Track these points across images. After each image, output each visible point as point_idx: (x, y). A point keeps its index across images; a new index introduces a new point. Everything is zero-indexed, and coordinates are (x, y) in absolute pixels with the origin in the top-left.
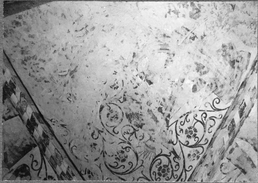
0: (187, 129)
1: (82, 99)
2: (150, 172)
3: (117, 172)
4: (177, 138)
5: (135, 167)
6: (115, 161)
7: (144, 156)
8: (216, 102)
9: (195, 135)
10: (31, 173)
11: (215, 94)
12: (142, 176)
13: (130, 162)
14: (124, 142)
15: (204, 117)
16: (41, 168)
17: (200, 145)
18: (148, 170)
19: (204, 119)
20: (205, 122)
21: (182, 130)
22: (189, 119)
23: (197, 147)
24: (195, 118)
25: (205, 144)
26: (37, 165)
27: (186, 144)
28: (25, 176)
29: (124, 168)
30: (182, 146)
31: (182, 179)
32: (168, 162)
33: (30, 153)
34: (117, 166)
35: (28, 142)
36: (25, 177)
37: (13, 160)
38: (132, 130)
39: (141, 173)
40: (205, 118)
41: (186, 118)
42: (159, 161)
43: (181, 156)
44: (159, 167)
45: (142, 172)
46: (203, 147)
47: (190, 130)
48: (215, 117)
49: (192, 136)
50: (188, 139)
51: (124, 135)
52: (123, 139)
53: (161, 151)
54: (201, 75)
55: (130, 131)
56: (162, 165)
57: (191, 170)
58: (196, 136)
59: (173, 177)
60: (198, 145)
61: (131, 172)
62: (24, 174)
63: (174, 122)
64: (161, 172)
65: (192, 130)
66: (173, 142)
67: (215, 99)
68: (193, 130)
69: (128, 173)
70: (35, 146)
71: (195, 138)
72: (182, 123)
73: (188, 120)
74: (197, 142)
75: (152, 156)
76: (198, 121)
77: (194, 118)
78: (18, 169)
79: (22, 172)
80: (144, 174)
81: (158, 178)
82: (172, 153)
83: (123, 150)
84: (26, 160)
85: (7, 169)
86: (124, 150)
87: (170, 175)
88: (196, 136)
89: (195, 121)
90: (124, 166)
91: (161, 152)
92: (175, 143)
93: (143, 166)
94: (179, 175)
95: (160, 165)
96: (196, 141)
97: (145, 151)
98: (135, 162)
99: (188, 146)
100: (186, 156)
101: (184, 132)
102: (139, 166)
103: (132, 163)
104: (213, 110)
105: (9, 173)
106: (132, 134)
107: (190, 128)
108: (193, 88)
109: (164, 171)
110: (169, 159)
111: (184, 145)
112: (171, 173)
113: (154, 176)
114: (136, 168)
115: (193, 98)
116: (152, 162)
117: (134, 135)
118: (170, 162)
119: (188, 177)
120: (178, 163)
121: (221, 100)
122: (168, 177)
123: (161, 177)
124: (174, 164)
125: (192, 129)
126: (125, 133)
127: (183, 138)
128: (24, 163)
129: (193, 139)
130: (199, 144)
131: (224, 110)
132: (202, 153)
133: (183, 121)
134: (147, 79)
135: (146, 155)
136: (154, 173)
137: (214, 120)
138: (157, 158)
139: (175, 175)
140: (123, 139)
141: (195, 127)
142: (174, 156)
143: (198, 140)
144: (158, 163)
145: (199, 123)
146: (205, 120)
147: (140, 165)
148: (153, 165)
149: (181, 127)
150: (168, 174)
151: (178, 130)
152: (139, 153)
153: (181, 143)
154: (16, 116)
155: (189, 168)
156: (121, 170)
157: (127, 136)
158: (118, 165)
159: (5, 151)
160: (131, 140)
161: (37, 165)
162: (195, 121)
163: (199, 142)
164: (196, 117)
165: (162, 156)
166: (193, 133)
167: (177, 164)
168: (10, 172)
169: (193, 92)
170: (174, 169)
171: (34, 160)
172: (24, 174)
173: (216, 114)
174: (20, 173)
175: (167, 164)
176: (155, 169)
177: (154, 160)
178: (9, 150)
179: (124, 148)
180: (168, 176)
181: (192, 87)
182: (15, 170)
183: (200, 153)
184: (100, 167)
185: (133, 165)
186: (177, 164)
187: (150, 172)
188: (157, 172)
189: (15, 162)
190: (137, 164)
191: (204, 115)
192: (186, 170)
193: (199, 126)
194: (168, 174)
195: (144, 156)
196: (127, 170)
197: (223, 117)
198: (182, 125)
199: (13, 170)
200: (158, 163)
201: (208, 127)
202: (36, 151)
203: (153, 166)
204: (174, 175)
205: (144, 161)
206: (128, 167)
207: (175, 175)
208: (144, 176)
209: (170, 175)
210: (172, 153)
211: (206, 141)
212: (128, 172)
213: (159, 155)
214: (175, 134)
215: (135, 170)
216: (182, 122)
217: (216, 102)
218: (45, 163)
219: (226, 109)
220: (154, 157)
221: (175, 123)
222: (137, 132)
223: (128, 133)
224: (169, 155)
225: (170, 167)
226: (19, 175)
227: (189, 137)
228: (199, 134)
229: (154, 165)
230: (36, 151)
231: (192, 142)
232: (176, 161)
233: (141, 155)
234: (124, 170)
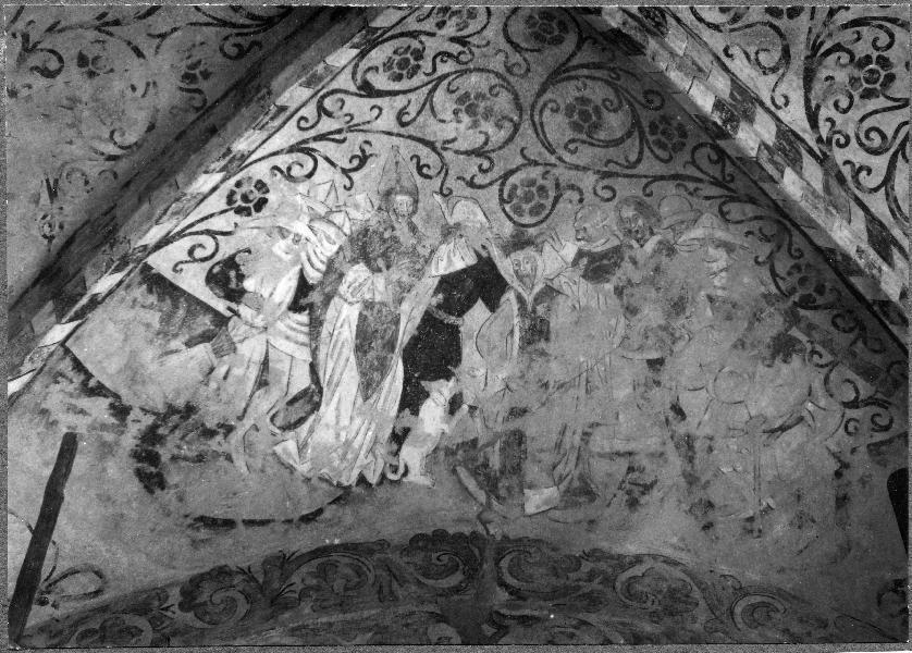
10: (227, 256)
16: (208, 232)
26: (201, 245)
28: (236, 267)
33: (169, 275)
35: (139, 292)
36: (242, 268)
62: (232, 274)
70: (147, 268)
78: (222, 294)
79: (228, 279)
84: (193, 281)
85: (231, 324)
105: (239, 316)
128: (204, 283)
159: (184, 347)
161: (201, 245)
168: (236, 313)
171: (189, 259)
172: (232, 274)
174: (233, 285)
178: (175, 336)
182: (228, 303)
184: (163, 36)
189: (208, 309)
199: (229, 309)
218: (192, 225)
226: (238, 286)
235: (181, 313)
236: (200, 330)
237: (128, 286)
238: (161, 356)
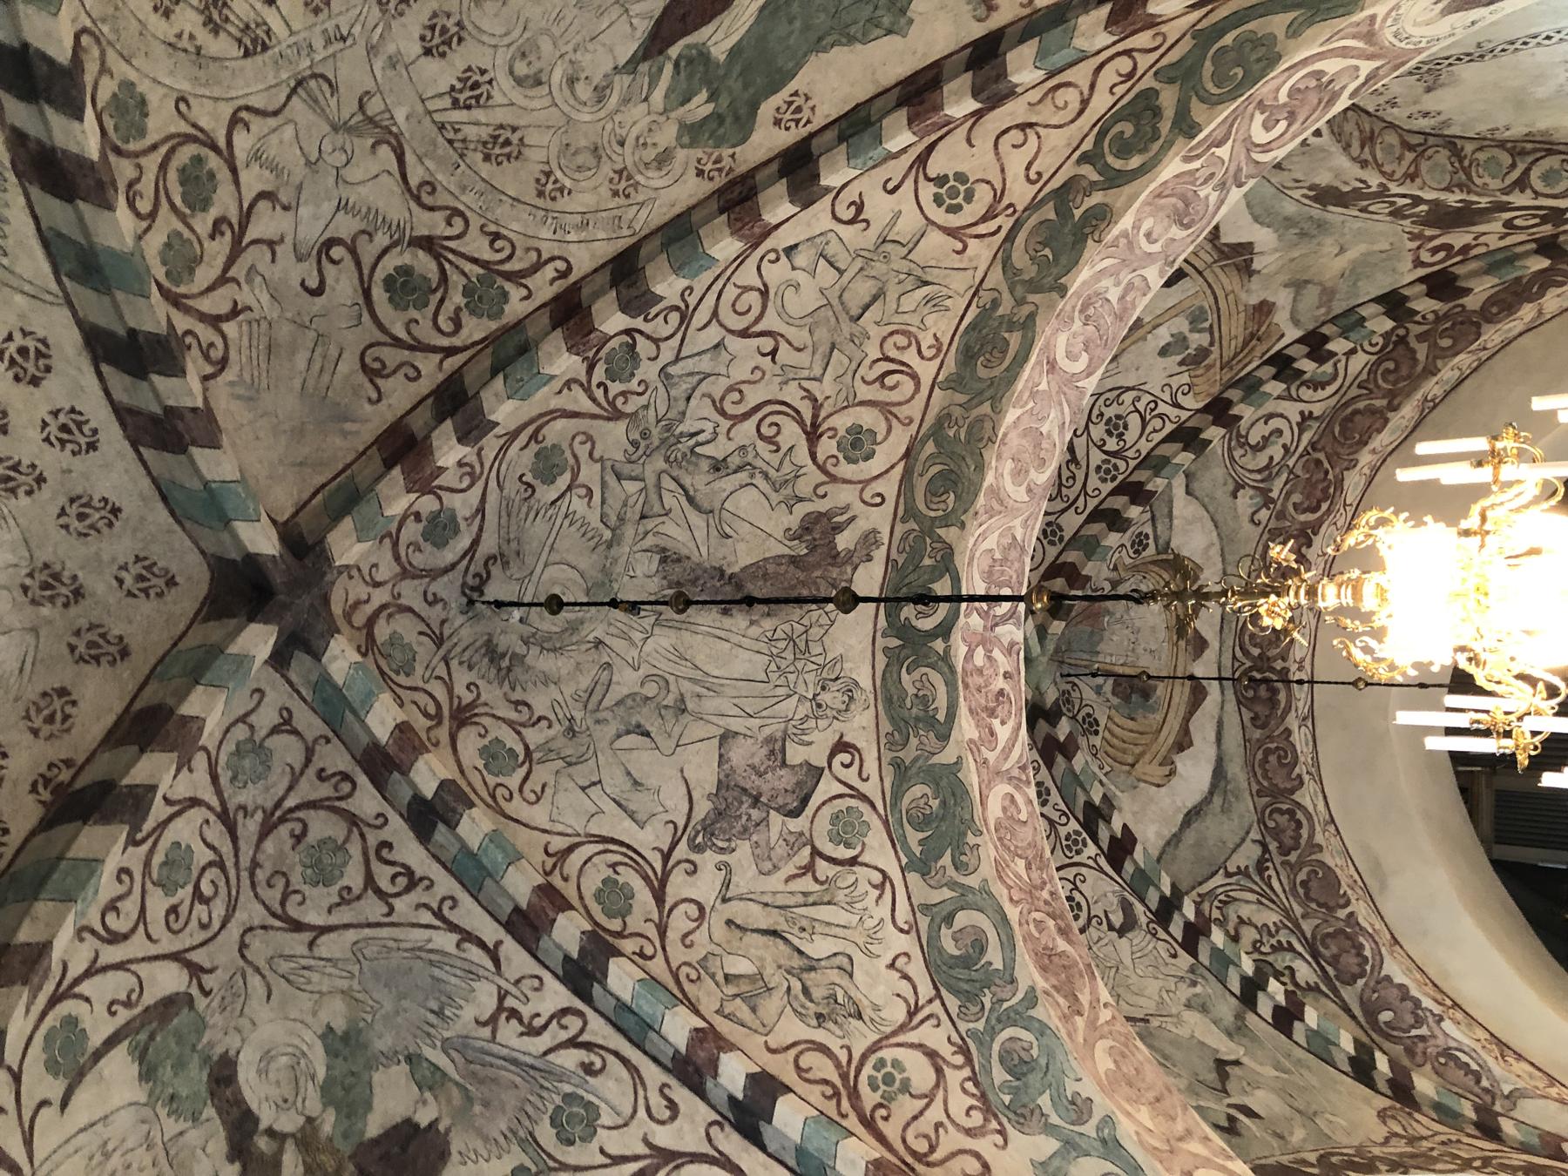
21: (1101, 415)
43: (1084, 464)
50: (1105, 437)
54: (1191, 331)
76: (1137, 411)
94: (1072, 498)
100: (1093, 466)
107: (1118, 417)
119: (1090, 508)
129: (1114, 440)
149: (1103, 409)
151: (1095, 412)
173: (1172, 412)
181: (1162, 343)
191: (1152, 405)
192: (1086, 494)
193: (1134, 421)
201: (1149, 429)
227: (1109, 433)
228: (1131, 435)
231: (1112, 445)
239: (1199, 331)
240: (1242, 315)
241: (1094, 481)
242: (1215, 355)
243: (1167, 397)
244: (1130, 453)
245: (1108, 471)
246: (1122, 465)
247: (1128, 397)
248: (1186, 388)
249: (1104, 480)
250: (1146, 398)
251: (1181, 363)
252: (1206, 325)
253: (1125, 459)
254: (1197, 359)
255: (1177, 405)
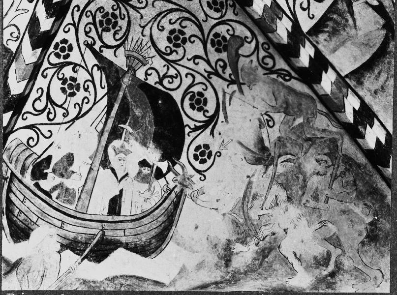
0: (78, 91)
1: (249, 121)
2: (129, 18)
3: (179, 12)
4: (92, 75)
5: (153, 23)
6: (185, 30)
7: (141, 43)
8: (33, 141)
9: (64, 81)
11: (36, 153)
12: (142, 11)
13: (161, 31)
14: (174, 62)
15: (52, 114)
17: (55, 68)
18: (133, 21)
19: (52, 111)
20: (49, 106)
21: (86, 90)
22: (75, 108)
23: (59, 64)
24: (65, 111)
25: (47, 69)
26: (301, 4)
27: (77, 67)
29: (171, 20)
30: (83, 64)
31: (78, 10)
32: (103, 37)
33: (315, 21)
34: (182, 21)
35: (322, 37)
37: (339, 6)
38: (166, 82)
39: (144, 16)
40: (49, 113)
41: (80, 110)
42: (118, 37)
43: (83, 47)
44: (117, 28)
45: (142, 17)
46: (50, 63)
47: (72, 91)
48: (34, 115)
49: (69, 80)
50: (74, 75)
51: (176, 72)
52: (177, 67)
53: (117, 54)
55: (169, 81)
56: (112, 31)
57: (66, 26)
58: (62, 81)
59: (94, 14)
60: (57, 67)
61: (158, 15)
63: (100, 102)
64: (113, 21)
65: (69, 91)
66: (98, 70)
67: (36, 145)
68: (67, 92)
69: (164, 12)
70: (309, 32)
71: (63, 78)
72: (86, 100)
73: (77, 106)
74: (59, 72)
75: (129, 45)
76: (61, 106)
77: (67, 111)
80: (138, 14)
81: (116, 10)
82: (98, 51)
83: (175, 49)
86: (174, 49)
87: (99, 17)
88: (62, 81)
89: (65, 106)
90: (171, 23)
91: (115, 52)
92: (95, 68)
93: (141, 27)
95: (115, 30)
96: (61, 72)
97: (141, 50)
98: (155, 31)
99: (73, 65)
101: (82, 86)
102: (148, 26)
103: (159, 30)
104: (38, 126)
106: (165, 76)
107: (73, 95)
108: (73, 160)
109: (108, 22)
110: (102, 42)
111: (80, 66)
112: (97, 20)
113: (122, 12)
114: (151, 23)
115: (72, 143)
116: (128, 35)
117: (161, 75)
118: (100, 38)
120: (87, 36)
121: (26, 145)
122: (101, 12)
123: (111, 11)
124: (93, 34)
125: (70, 93)
126: (175, 76)
127: (82, 76)
128: (322, 3)
129: (67, 76)
130: (56, 69)
131: (20, 128)
132: (51, 54)
133: (84, 104)
134: (149, 169)
135: (139, 44)
136: (123, 17)
137: (35, 109)
138: (121, 41)
139: (89, 16)
140: (177, 67)
141: (66, 95)
142: (94, 47)
143: (58, 74)
144: (118, 34)
145: (59, 104)
146: (49, 108)
147: (146, 28)
148: (126, 30)
149: (87, 94)
150: (100, 18)
151: (91, 89)
152: (150, 47)
153: (85, 67)
154: (347, 76)
155: (69, 28)
156: (174, 16)
157: (172, 72)
158: (180, 24)
160: (164, 66)
161: (301, 4)
162: (65, 106)
163: (58, 72)
164: (64, 113)
165: (113, 45)
166: (68, 85)
167: (88, 35)
169: (72, 154)
170: (92, 27)
171: (307, 11)
173: (31, 120)
175: (104, 33)
176: (123, 23)
177: (126, 39)
178: (347, 21)
179: (175, 53)
180: (102, 14)
183: (53, 54)
184: (206, 15)
185: (156, 26)
186: (88, 35)
187: (129, 18)
188: (119, 20)
190: (151, 29)
191: (51, 116)
192: (74, 25)
193: (58, 96)
194: (100, 18)
195: (141, 43)
196: (165, 18)
197: (21, 117)
198: (86, 97)
200: (118, 34)
201: (44, 98)
202: (306, 25)
203: (125, 28)
204: (91, 17)
205: (140, 34)
206: (165, 22)
207: (89, 16)
208: (138, 12)
209: (99, 17)
210: (98, 51)
211: (45, 74)
212: (163, 15)
213: (118, 47)
214: (96, 82)
215: (153, 18)
216: (87, 103)
217: (33, 141)
218: (290, 8)
219: (17, 130)
220: (126, 42)
221: (97, 100)
222: (157, 80)
223: (171, 77)
224: (102, 49)
225: (100, 30)
227: (73, 79)
228: (57, 85)
229: (124, 30)
230: (306, 25)
231: (67, 72)
232: (91, 40)
233: (146, 44)
234: (170, 16)
235: (335, 16)
236: (346, 8)
237: (317, 42)
238: (356, 29)
239: (55, 188)
240: (34, 219)
241: (71, 37)
242: (28, 179)
243: (44, 129)
244: (50, 72)
245: (63, 49)
246: (54, 60)
247: (73, 112)
248: (31, 142)
249: (65, 41)
250: (59, 118)
251: (49, 158)
252: (54, 195)
253: (53, 66)
254: (39, 170)
255: (31, 127)
